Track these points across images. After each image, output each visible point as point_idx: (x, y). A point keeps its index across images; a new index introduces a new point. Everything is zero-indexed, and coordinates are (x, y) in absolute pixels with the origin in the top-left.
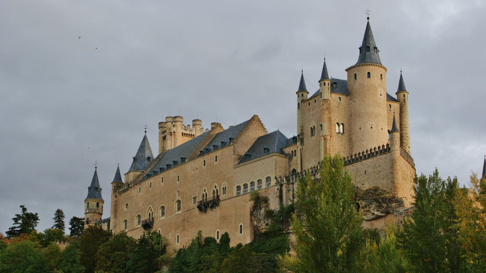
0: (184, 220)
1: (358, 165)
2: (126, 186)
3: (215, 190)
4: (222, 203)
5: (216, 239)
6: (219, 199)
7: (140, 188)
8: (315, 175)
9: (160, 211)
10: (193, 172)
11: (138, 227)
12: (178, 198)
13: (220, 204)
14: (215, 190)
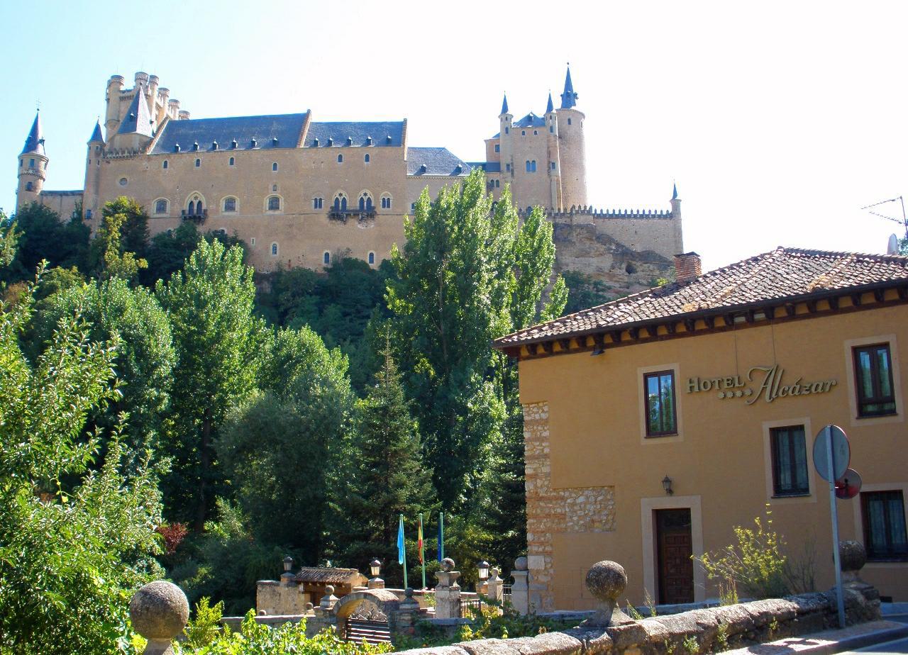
0: (291, 226)
1: (625, 221)
2: (129, 153)
3: (365, 199)
4: (379, 218)
5: (368, 261)
6: (376, 212)
7: (166, 162)
8: (554, 218)
9: (223, 204)
10: (313, 165)
11: (158, 216)
12: (275, 194)
13: (376, 217)
14: (365, 199)
